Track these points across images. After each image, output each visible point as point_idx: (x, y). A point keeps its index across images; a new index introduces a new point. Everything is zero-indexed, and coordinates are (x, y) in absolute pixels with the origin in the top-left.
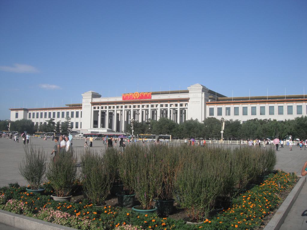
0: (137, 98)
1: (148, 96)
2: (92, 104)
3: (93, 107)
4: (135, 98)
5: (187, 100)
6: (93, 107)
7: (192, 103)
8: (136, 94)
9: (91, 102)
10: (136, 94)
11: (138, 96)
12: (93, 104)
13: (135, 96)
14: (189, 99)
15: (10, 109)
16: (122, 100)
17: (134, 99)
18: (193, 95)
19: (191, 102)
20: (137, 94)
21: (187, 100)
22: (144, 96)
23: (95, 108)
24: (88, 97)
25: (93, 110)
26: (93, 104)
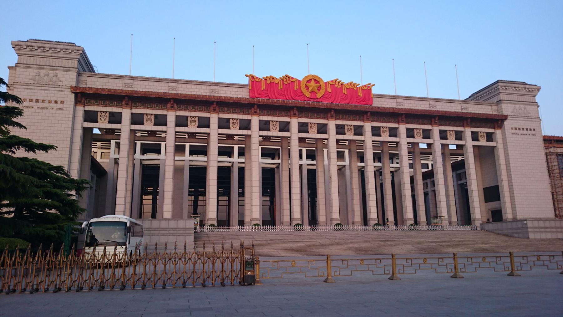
0: (319, 95)
1: (360, 94)
3: (80, 110)
4: (308, 95)
5: (497, 121)
6: (80, 110)
7: (514, 131)
9: (74, 84)
10: (313, 81)
14: (506, 119)
16: (248, 97)
18: (515, 108)
19: (512, 129)
20: (317, 81)
21: (497, 121)
23: (90, 117)
24: (64, 63)
25: (80, 124)
26: (82, 96)
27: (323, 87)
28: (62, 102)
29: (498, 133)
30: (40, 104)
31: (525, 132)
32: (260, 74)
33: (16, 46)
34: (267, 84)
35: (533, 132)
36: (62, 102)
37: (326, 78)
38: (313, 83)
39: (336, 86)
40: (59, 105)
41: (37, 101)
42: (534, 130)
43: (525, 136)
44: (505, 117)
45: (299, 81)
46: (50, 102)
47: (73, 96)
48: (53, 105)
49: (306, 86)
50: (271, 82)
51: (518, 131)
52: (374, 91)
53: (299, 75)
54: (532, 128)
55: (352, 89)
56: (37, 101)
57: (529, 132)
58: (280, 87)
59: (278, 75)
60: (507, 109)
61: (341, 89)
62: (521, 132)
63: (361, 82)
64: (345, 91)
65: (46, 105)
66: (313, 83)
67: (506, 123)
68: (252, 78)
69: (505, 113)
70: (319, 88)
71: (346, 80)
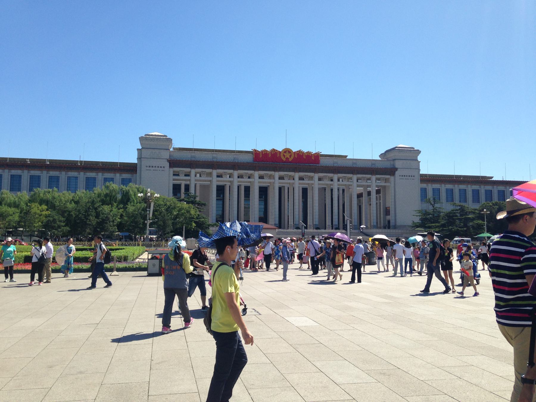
0: (290, 160)
1: (313, 158)
2: (170, 163)
3: (172, 170)
4: (284, 159)
5: (392, 171)
7: (401, 177)
8: (287, 152)
10: (287, 152)
11: (292, 157)
12: (173, 163)
13: (284, 156)
17: (283, 161)
21: (392, 171)
22: (304, 157)
28: (164, 167)
29: (392, 178)
30: (154, 168)
31: (408, 177)
34: (262, 154)
35: (413, 178)
36: (164, 167)
37: (294, 149)
39: (300, 154)
40: (163, 169)
41: (152, 167)
44: (396, 169)
45: (280, 152)
46: (158, 167)
47: (168, 164)
48: (159, 169)
50: (265, 153)
51: (403, 177)
53: (280, 148)
55: (309, 155)
56: (152, 167)
57: (410, 177)
58: (270, 156)
59: (269, 149)
60: (398, 164)
62: (406, 177)
63: (314, 151)
64: (304, 157)
65: (157, 168)
67: (397, 173)
68: (255, 150)
69: (396, 167)
70: (290, 156)
71: (305, 150)
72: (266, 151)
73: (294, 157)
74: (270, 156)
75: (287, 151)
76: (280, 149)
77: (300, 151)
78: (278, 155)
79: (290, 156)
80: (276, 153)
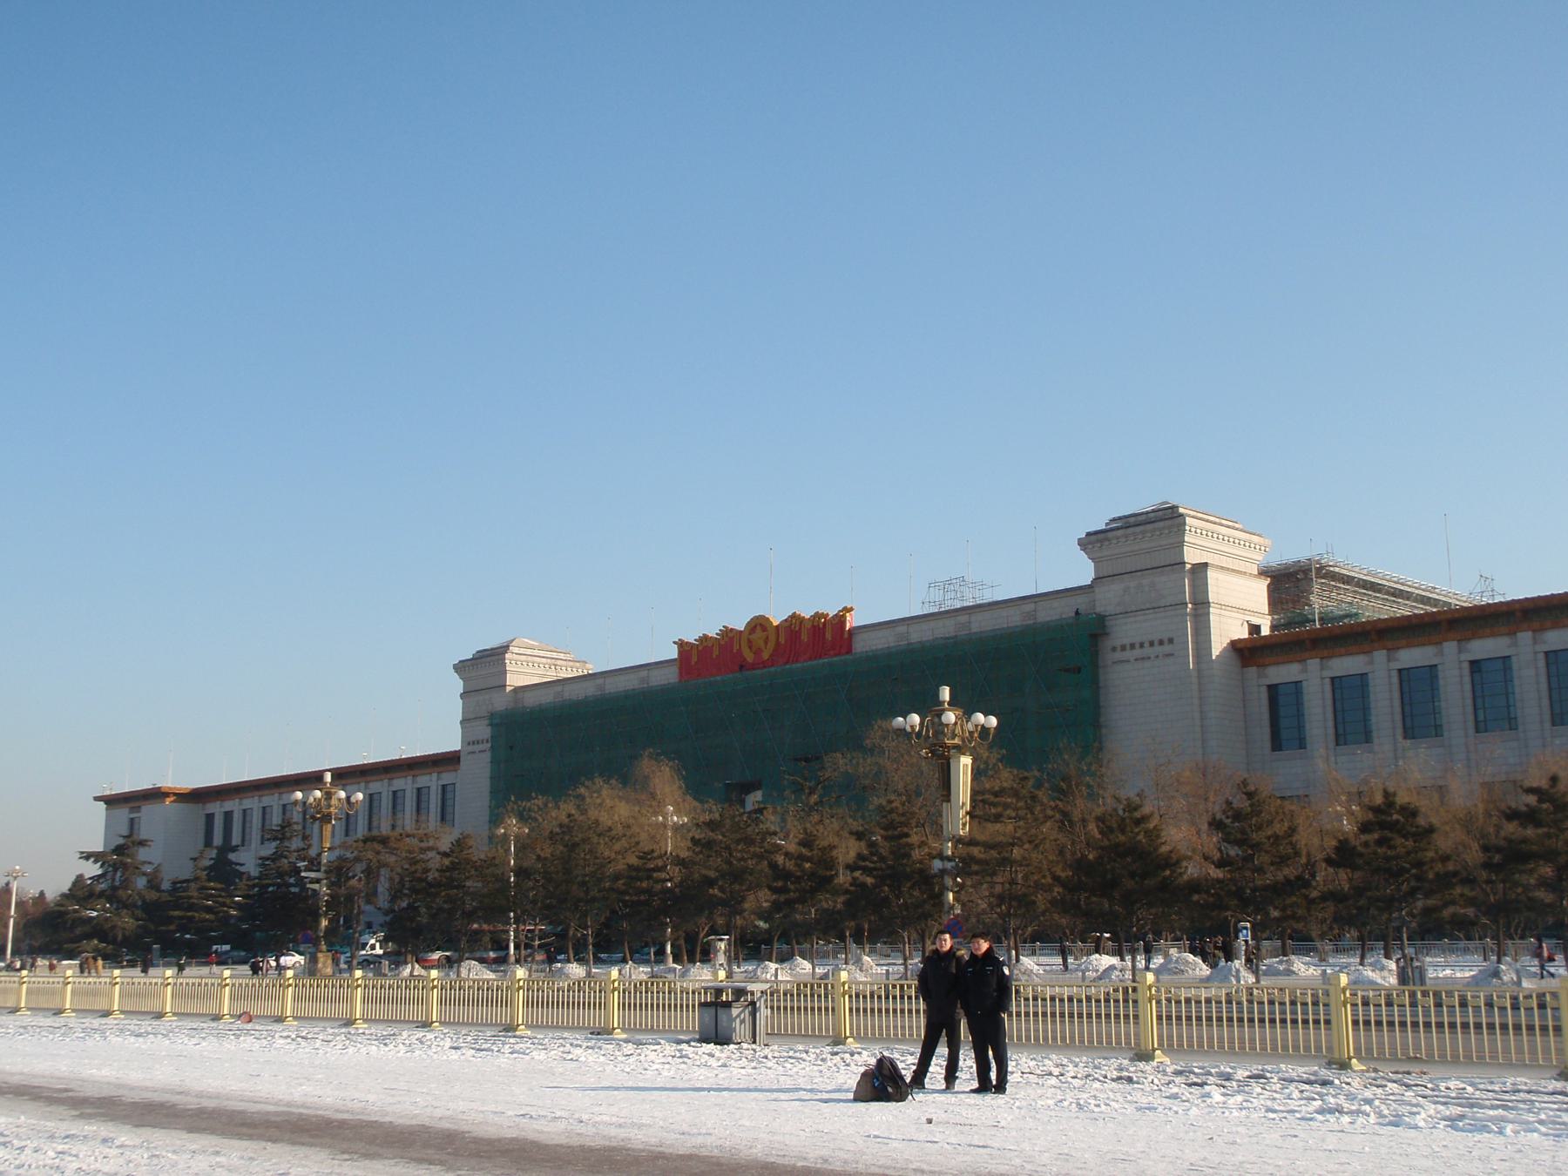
0: (766, 655)
4: (749, 657)
11: (771, 645)
15: (97, 799)
20: (764, 629)
27: (772, 638)
31: (1148, 651)
32: (691, 637)
33: (461, 668)
35: (1167, 648)
38: (759, 633)
42: (1171, 641)
43: (1147, 664)
49: (750, 641)
52: (852, 621)
54: (1165, 636)
57: (1158, 649)
58: (716, 653)
59: (713, 631)
61: (799, 632)
62: (1137, 652)
64: (804, 637)
66: (759, 633)
68: (681, 645)
70: (766, 641)
71: (807, 614)
72: (705, 637)
73: (778, 643)
74: (716, 653)
75: (759, 624)
76: (740, 626)
77: (794, 616)
78: (736, 647)
79: (766, 641)
80: (732, 639)
